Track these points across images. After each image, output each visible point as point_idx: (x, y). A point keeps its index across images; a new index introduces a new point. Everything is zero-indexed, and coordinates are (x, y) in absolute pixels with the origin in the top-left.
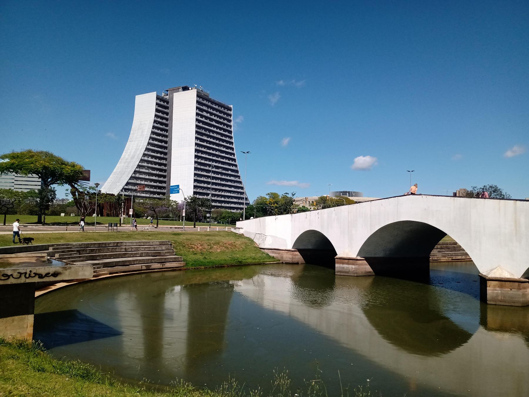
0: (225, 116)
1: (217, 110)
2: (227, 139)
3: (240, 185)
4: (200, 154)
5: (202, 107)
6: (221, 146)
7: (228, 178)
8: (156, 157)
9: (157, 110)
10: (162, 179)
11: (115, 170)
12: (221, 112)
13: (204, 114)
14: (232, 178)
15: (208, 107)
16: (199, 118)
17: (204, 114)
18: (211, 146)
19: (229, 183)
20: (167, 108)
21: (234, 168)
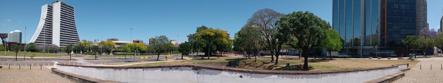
0: (72, 11)
1: (68, 9)
2: (73, 19)
3: (78, 37)
4: (62, 26)
5: (63, 8)
6: (70, 22)
7: (73, 34)
8: (48, 28)
9: (48, 10)
10: (50, 35)
11: (35, 33)
12: (70, 9)
13: (64, 10)
14: (75, 34)
15: (65, 7)
16: (62, 12)
17: (64, 10)
18: (66, 22)
19: (73, 36)
20: (52, 9)
21: (75, 30)
